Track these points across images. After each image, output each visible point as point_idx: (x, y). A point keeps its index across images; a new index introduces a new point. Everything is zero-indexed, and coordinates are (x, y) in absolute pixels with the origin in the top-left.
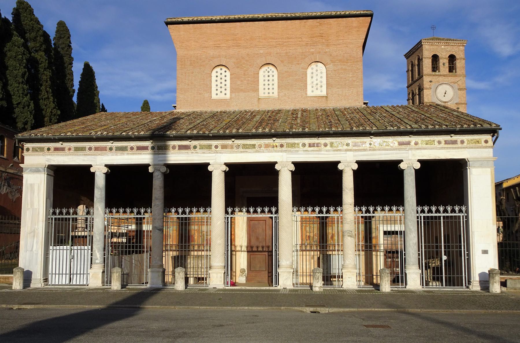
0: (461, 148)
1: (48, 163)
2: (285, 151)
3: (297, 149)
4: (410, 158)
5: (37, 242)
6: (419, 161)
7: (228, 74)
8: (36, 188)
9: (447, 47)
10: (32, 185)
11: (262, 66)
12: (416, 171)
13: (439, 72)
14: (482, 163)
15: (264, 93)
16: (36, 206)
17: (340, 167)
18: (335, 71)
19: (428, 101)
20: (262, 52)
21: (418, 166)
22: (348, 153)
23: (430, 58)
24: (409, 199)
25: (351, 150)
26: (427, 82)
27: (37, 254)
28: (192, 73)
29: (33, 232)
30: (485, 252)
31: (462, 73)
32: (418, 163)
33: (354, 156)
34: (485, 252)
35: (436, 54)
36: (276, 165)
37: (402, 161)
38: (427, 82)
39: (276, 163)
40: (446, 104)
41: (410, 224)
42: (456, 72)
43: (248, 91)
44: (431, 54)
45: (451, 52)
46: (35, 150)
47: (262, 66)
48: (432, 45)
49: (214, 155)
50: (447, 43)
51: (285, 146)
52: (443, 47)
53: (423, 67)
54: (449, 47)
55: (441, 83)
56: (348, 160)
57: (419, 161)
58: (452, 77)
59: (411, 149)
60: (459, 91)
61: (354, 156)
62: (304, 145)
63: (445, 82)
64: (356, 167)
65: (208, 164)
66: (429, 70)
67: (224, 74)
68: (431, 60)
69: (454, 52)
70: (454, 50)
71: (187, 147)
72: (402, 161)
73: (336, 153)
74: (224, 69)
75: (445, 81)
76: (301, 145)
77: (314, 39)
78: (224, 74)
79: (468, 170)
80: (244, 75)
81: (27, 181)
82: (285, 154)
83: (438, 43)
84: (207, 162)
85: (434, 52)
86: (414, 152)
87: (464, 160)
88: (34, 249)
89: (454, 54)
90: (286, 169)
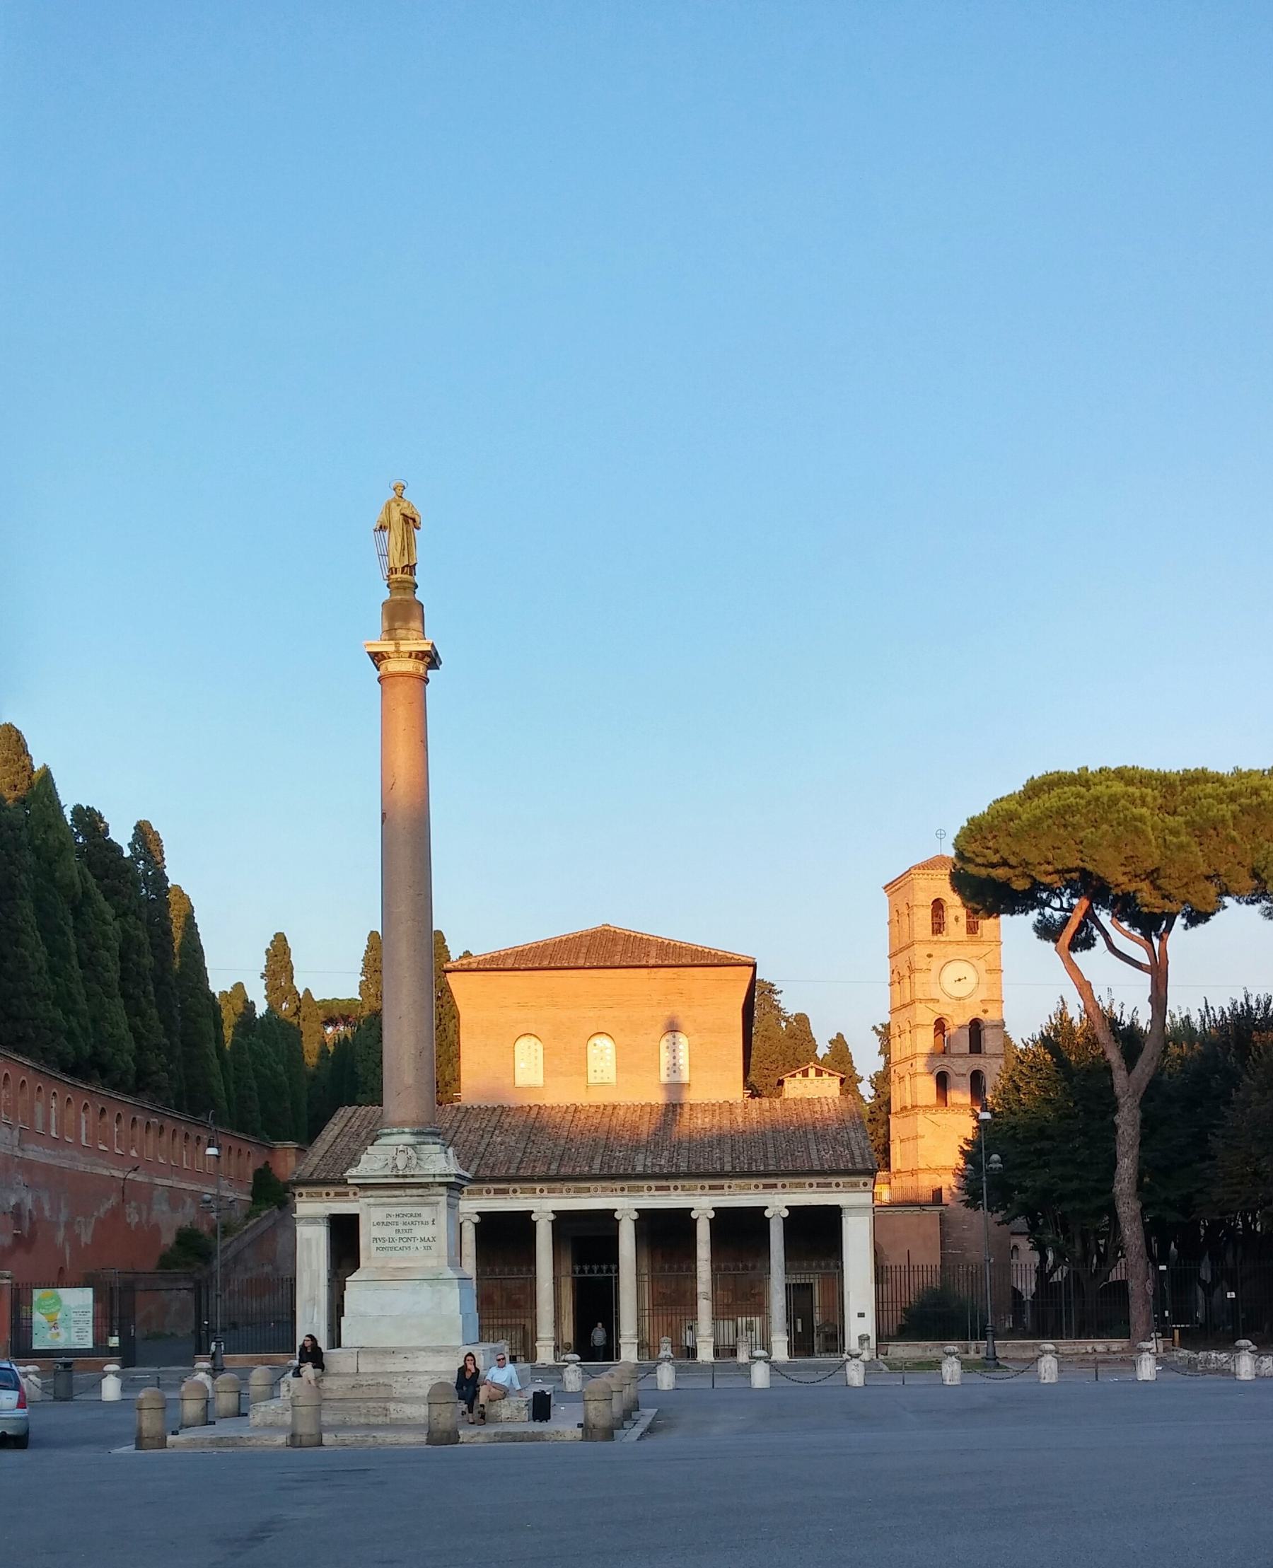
0: (836, 1192)
1: (327, 1213)
2: (627, 1196)
3: (641, 1193)
4: (777, 1204)
5: (318, 1313)
6: (787, 1207)
7: (540, 1047)
8: (314, 1243)
10: (308, 1240)
11: (594, 1035)
12: (784, 1219)
14: (858, 1209)
15: (595, 1078)
16: (314, 1267)
17: (694, 1215)
18: (701, 1044)
20: (591, 1014)
21: (786, 1213)
22: (703, 1197)
24: (775, 1253)
25: (706, 1195)
27: (319, 1327)
28: (486, 1045)
29: (313, 1300)
30: (861, 1315)
32: (787, 1210)
33: (710, 1201)
34: (861, 1315)
36: (616, 1213)
37: (766, 1208)
39: (616, 1210)
41: (775, 1283)
43: (572, 1075)
46: (310, 1195)
47: (594, 1035)
49: (539, 1200)
51: (626, 1190)
56: (704, 1206)
57: (787, 1207)
59: (778, 1194)
61: (710, 1201)
62: (650, 1189)
64: (712, 1215)
65: (532, 1212)
67: (533, 1047)
71: (505, 1192)
72: (766, 1208)
73: (688, 1197)
74: (534, 1039)
76: (645, 1188)
77: (669, 997)
78: (533, 1047)
79: (844, 1219)
80: (565, 1049)
81: (301, 1234)
82: (626, 1199)
84: (531, 1209)
86: (781, 1196)
87: (838, 1206)
88: (315, 1320)
90: (628, 1217)
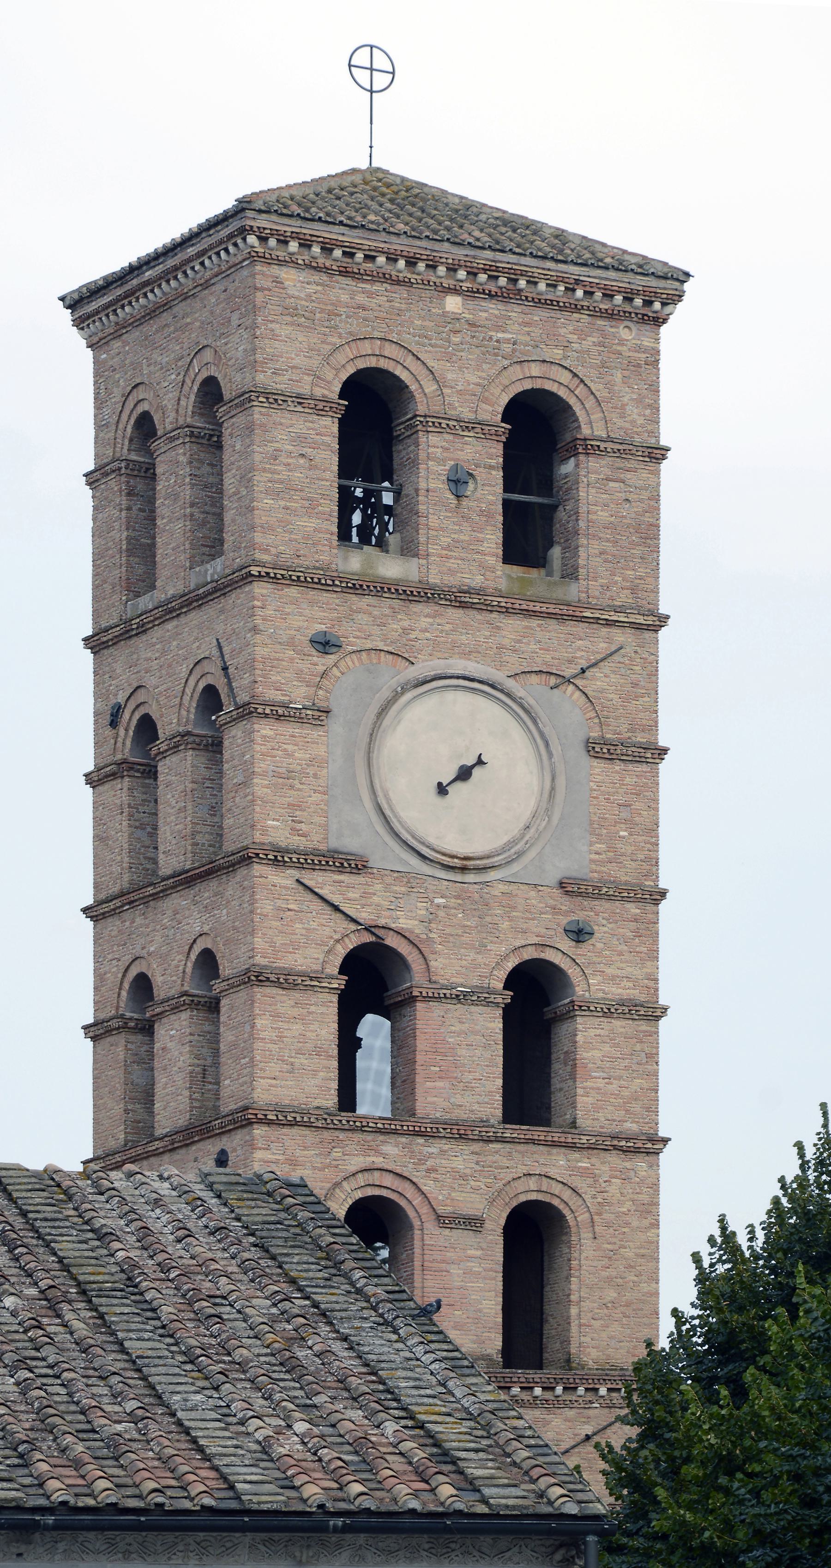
9: (493, 308)
13: (409, 550)
19: (296, 842)
23: (319, 407)
26: (291, 643)
31: (634, 590)
35: (383, 364)
38: (291, 643)
40: (470, 878)
42: (571, 574)
44: (340, 358)
45: (535, 370)
48: (344, 272)
50: (493, 274)
52: (453, 303)
53: (246, 480)
54: (515, 312)
55: (424, 667)
58: (534, 623)
60: (599, 766)
63: (460, 666)
66: (309, 524)
68: (330, 427)
69: (565, 377)
70: (557, 354)
75: (466, 655)
83: (411, 263)
85: (366, 347)
89: (562, 393)
